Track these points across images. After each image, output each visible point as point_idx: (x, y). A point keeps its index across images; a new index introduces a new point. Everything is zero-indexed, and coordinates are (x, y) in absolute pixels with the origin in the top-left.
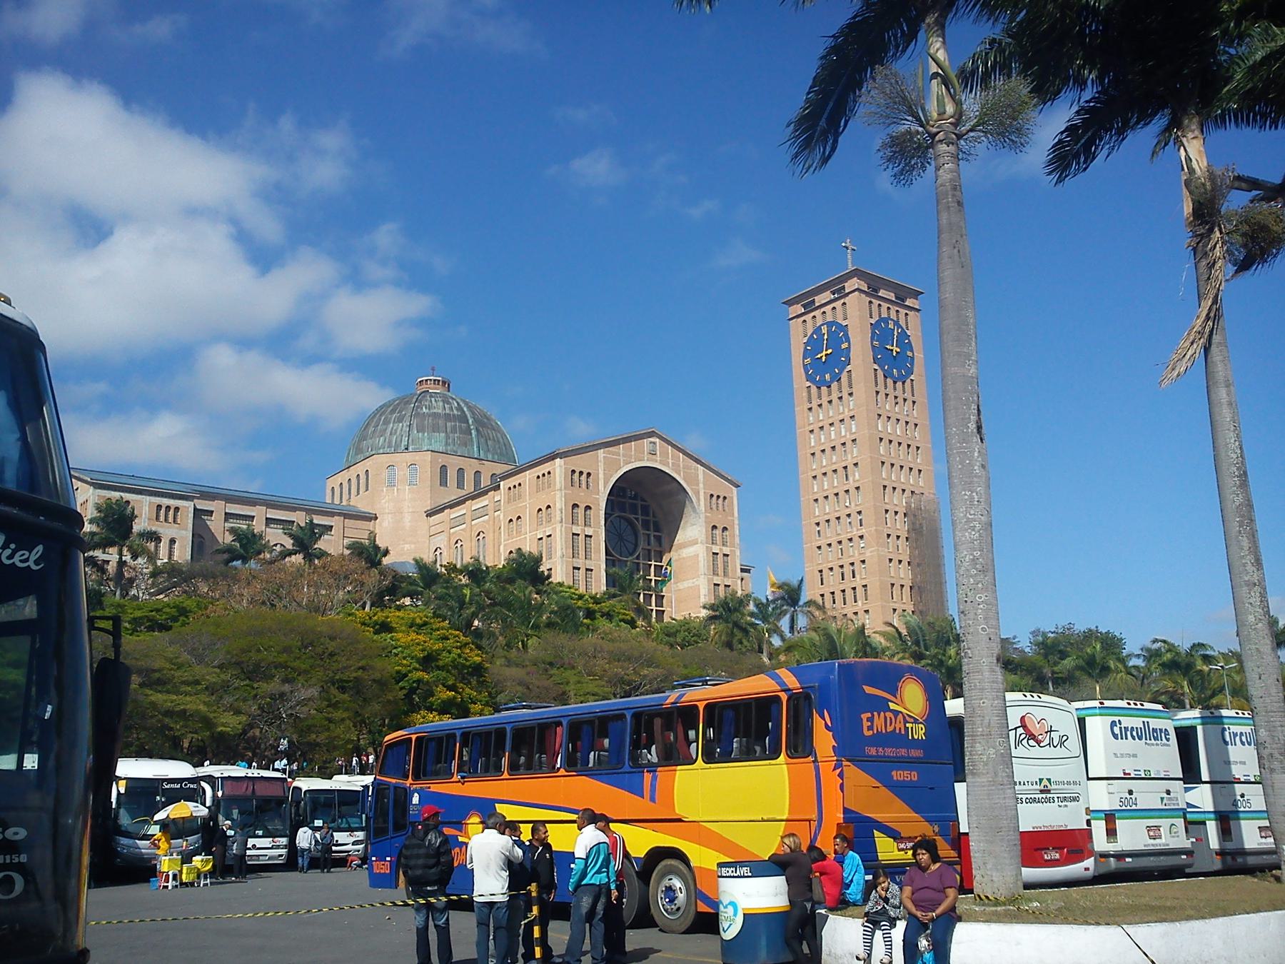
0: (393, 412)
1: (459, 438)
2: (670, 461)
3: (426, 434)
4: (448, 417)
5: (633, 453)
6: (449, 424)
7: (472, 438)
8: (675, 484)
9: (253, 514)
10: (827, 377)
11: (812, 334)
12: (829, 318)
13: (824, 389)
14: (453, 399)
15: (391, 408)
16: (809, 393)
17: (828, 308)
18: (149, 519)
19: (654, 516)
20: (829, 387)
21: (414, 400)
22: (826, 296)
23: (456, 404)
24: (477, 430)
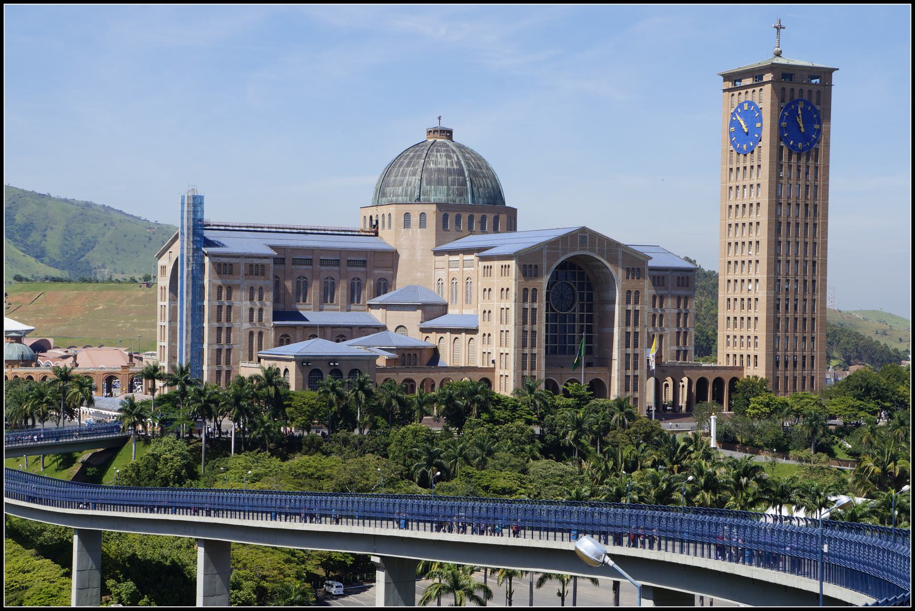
0: (408, 165)
1: (457, 189)
2: (597, 248)
3: (433, 187)
4: (449, 172)
5: (569, 247)
6: (450, 178)
7: (467, 189)
8: (600, 263)
9: (311, 257)
10: (745, 146)
11: (737, 108)
12: (749, 98)
13: (742, 156)
14: (454, 152)
15: (407, 161)
16: (731, 155)
17: (750, 90)
18: (245, 275)
19: (588, 279)
20: (745, 155)
21: (424, 155)
22: (748, 81)
23: (456, 158)
24: (471, 181)
